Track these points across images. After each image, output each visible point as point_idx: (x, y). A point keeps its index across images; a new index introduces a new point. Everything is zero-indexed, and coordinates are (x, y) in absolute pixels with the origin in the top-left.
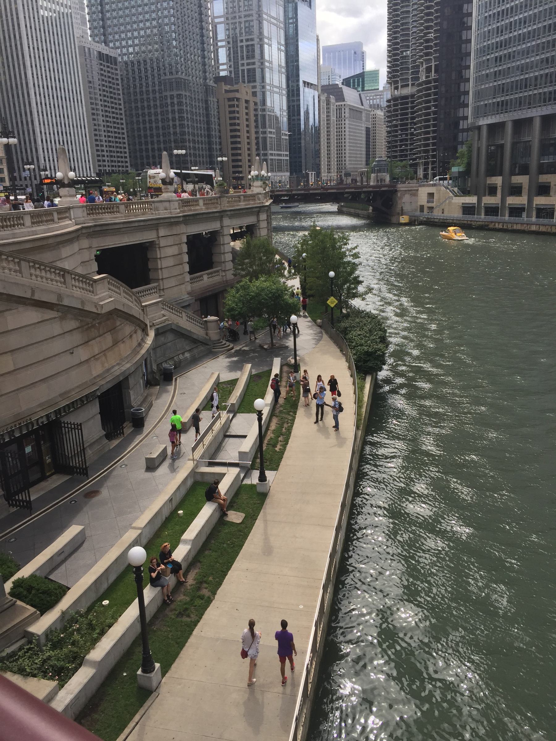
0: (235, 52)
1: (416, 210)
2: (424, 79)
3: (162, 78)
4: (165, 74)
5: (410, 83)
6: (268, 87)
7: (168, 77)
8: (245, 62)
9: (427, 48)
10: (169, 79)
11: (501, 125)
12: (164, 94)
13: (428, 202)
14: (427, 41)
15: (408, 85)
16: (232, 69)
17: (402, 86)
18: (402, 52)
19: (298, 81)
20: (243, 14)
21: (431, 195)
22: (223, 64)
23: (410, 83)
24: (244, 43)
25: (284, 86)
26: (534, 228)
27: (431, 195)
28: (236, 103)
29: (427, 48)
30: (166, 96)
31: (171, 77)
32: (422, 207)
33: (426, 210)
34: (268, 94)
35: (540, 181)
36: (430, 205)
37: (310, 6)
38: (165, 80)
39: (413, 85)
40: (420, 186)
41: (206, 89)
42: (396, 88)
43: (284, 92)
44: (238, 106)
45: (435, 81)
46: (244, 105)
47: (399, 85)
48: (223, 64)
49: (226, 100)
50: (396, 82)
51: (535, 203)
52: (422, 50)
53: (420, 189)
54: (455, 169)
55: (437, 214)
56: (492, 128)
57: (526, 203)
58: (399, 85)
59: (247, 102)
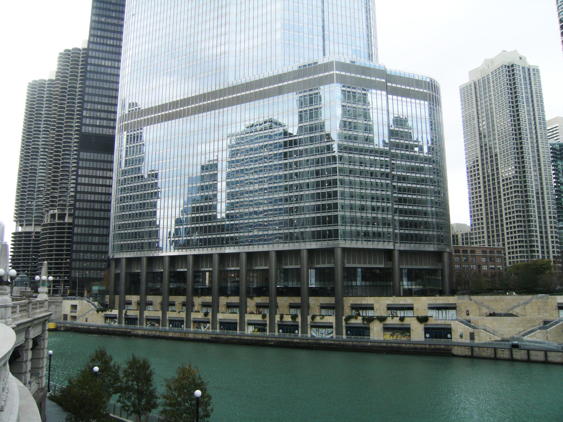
1: (60, 318)
2: (49, 222)
5: (33, 223)
9: (52, 201)
11: (139, 259)
13: (71, 312)
14: (53, 197)
15: (31, 225)
17: (26, 225)
18: (28, 202)
21: (74, 307)
23: (33, 223)
26: (170, 335)
27: (74, 307)
29: (52, 201)
32: (65, 317)
33: (69, 318)
35: (170, 300)
36: (73, 314)
39: (35, 225)
40: (64, 299)
42: (22, 225)
45: (59, 224)
47: (24, 223)
50: (20, 221)
51: (168, 316)
52: (48, 203)
53: (64, 301)
54: (95, 288)
55: (80, 321)
56: (129, 261)
57: (138, 314)
58: (24, 223)
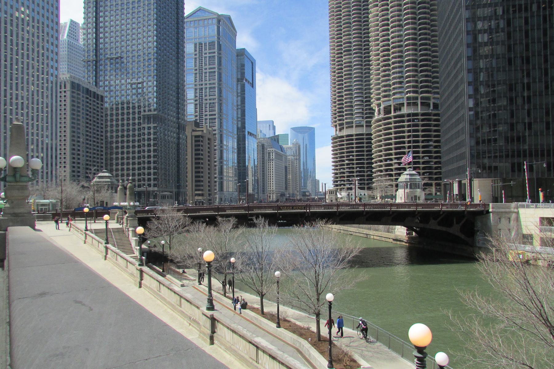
0: (201, 109)
3: (142, 114)
4: (145, 111)
6: (225, 132)
7: (147, 113)
8: (208, 113)
10: (147, 115)
12: (143, 125)
16: (198, 118)
19: (245, 131)
20: (208, 82)
22: (191, 103)
24: (208, 102)
25: (236, 133)
28: (201, 139)
30: (144, 128)
31: (150, 113)
34: (224, 136)
37: (253, 87)
38: (143, 115)
41: (179, 126)
43: (236, 137)
44: (202, 141)
46: (207, 141)
48: (191, 103)
49: (193, 137)
59: (209, 139)
